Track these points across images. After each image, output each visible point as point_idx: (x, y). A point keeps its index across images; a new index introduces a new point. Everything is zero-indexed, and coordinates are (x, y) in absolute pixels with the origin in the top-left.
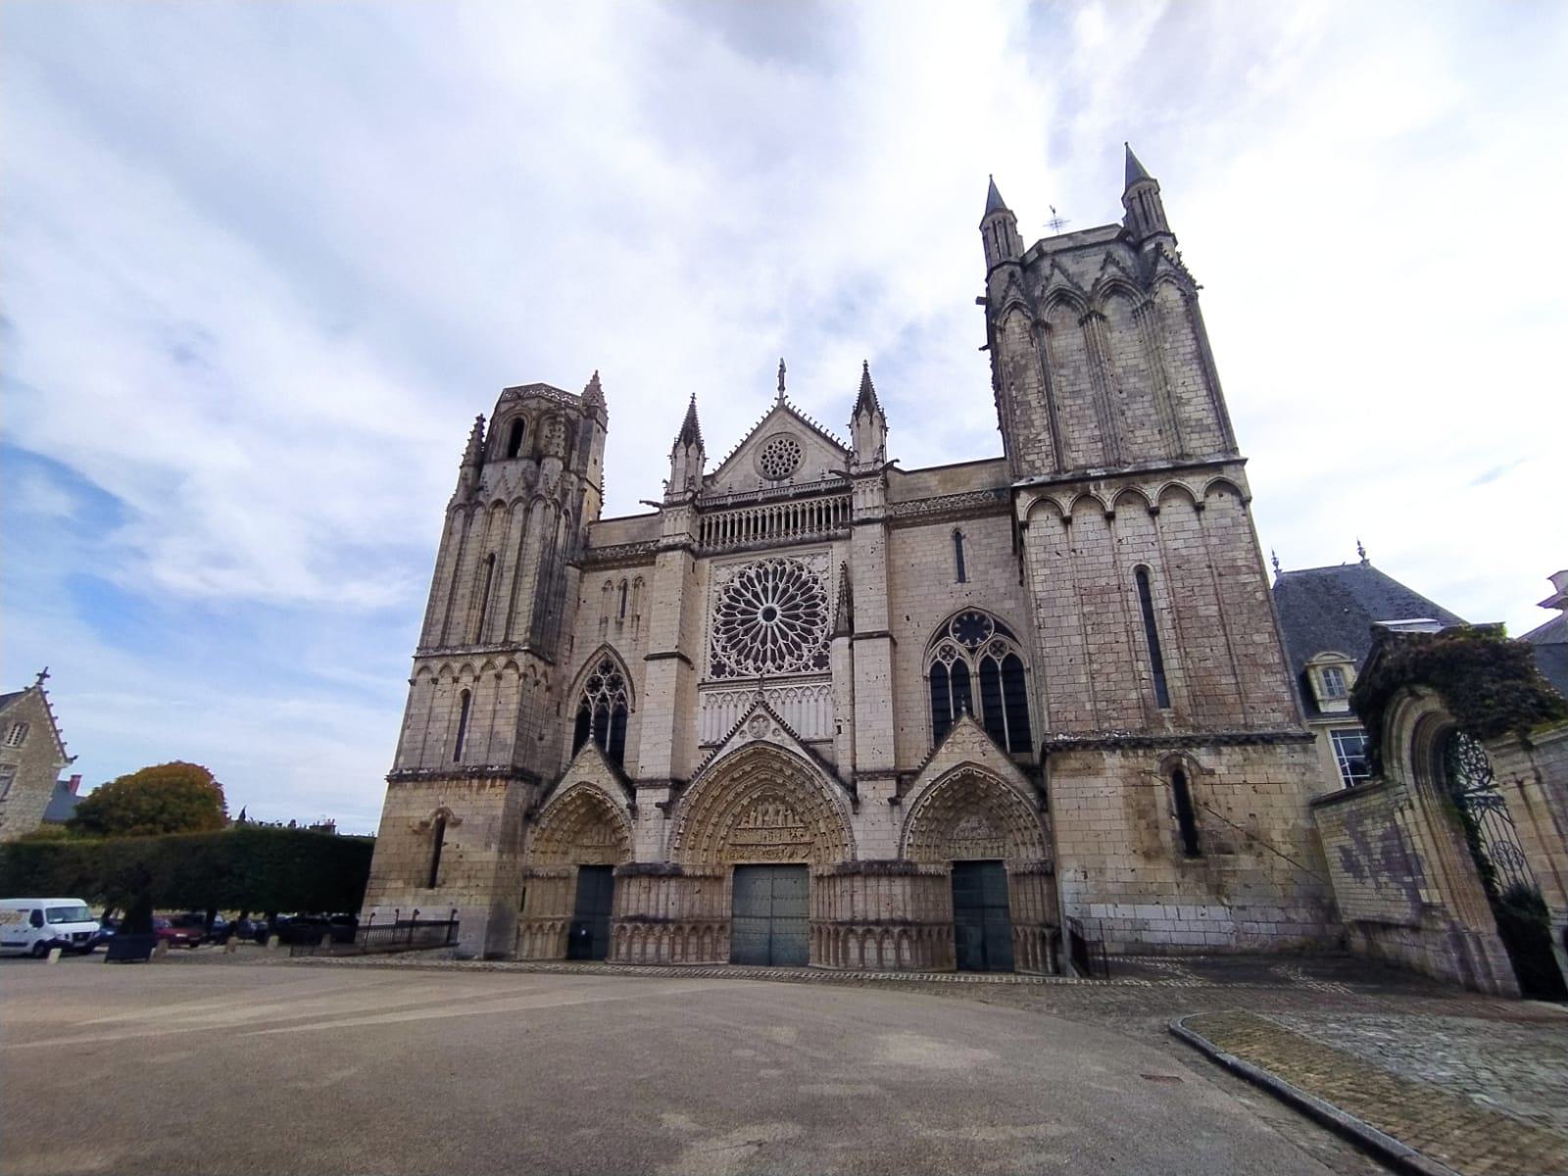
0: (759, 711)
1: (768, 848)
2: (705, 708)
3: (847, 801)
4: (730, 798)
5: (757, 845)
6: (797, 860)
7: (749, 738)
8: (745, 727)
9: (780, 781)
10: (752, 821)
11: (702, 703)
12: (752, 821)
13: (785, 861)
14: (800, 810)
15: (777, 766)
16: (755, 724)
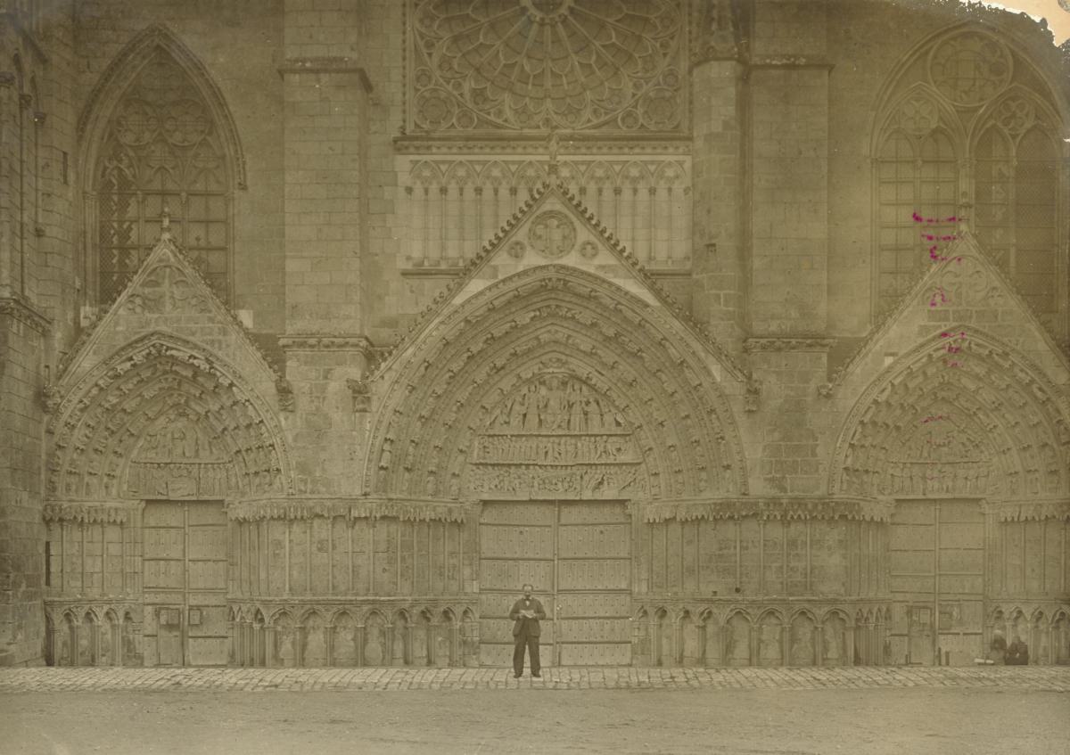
0: (553, 204)
1: (552, 472)
2: (409, 190)
3: (735, 388)
4: (480, 376)
5: (528, 466)
6: (609, 493)
7: (532, 259)
8: (521, 235)
9: (585, 347)
10: (515, 421)
11: (404, 179)
12: (515, 421)
13: (587, 495)
14: (621, 403)
15: (586, 317)
16: (540, 230)
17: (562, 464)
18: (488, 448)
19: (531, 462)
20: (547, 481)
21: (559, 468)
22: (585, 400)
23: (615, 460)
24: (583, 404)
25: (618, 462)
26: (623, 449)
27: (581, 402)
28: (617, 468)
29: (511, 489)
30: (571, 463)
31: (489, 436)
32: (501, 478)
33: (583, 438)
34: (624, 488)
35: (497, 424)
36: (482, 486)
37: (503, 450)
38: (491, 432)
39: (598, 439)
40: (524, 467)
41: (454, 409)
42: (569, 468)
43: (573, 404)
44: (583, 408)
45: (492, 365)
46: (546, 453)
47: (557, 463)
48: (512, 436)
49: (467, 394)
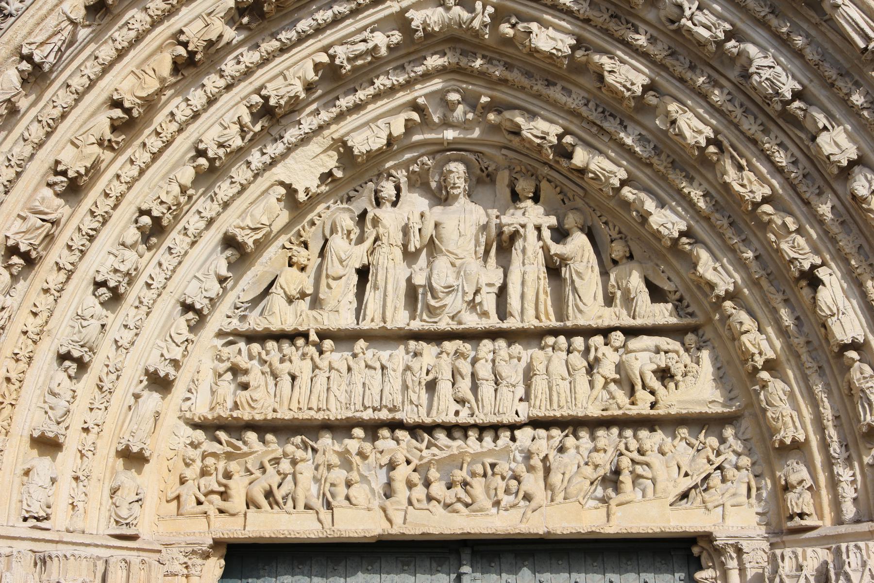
5: (372, 429)
17: (481, 418)
18: (246, 372)
19: (384, 415)
20: (433, 474)
21: (473, 435)
22: (553, 221)
23: (653, 406)
24: (547, 234)
25: (661, 411)
26: (677, 370)
27: (538, 228)
28: (659, 436)
29: (317, 503)
30: (509, 418)
31: (251, 337)
32: (285, 466)
33: (550, 340)
34: (685, 496)
35: (277, 299)
36: (224, 495)
37: (294, 378)
38: (256, 322)
39: (598, 340)
40: (358, 432)
41: (133, 235)
42: (505, 436)
43: (514, 236)
44: (546, 249)
45: (256, 99)
46: (431, 386)
47: (464, 417)
48: (323, 335)
49: (176, 190)
